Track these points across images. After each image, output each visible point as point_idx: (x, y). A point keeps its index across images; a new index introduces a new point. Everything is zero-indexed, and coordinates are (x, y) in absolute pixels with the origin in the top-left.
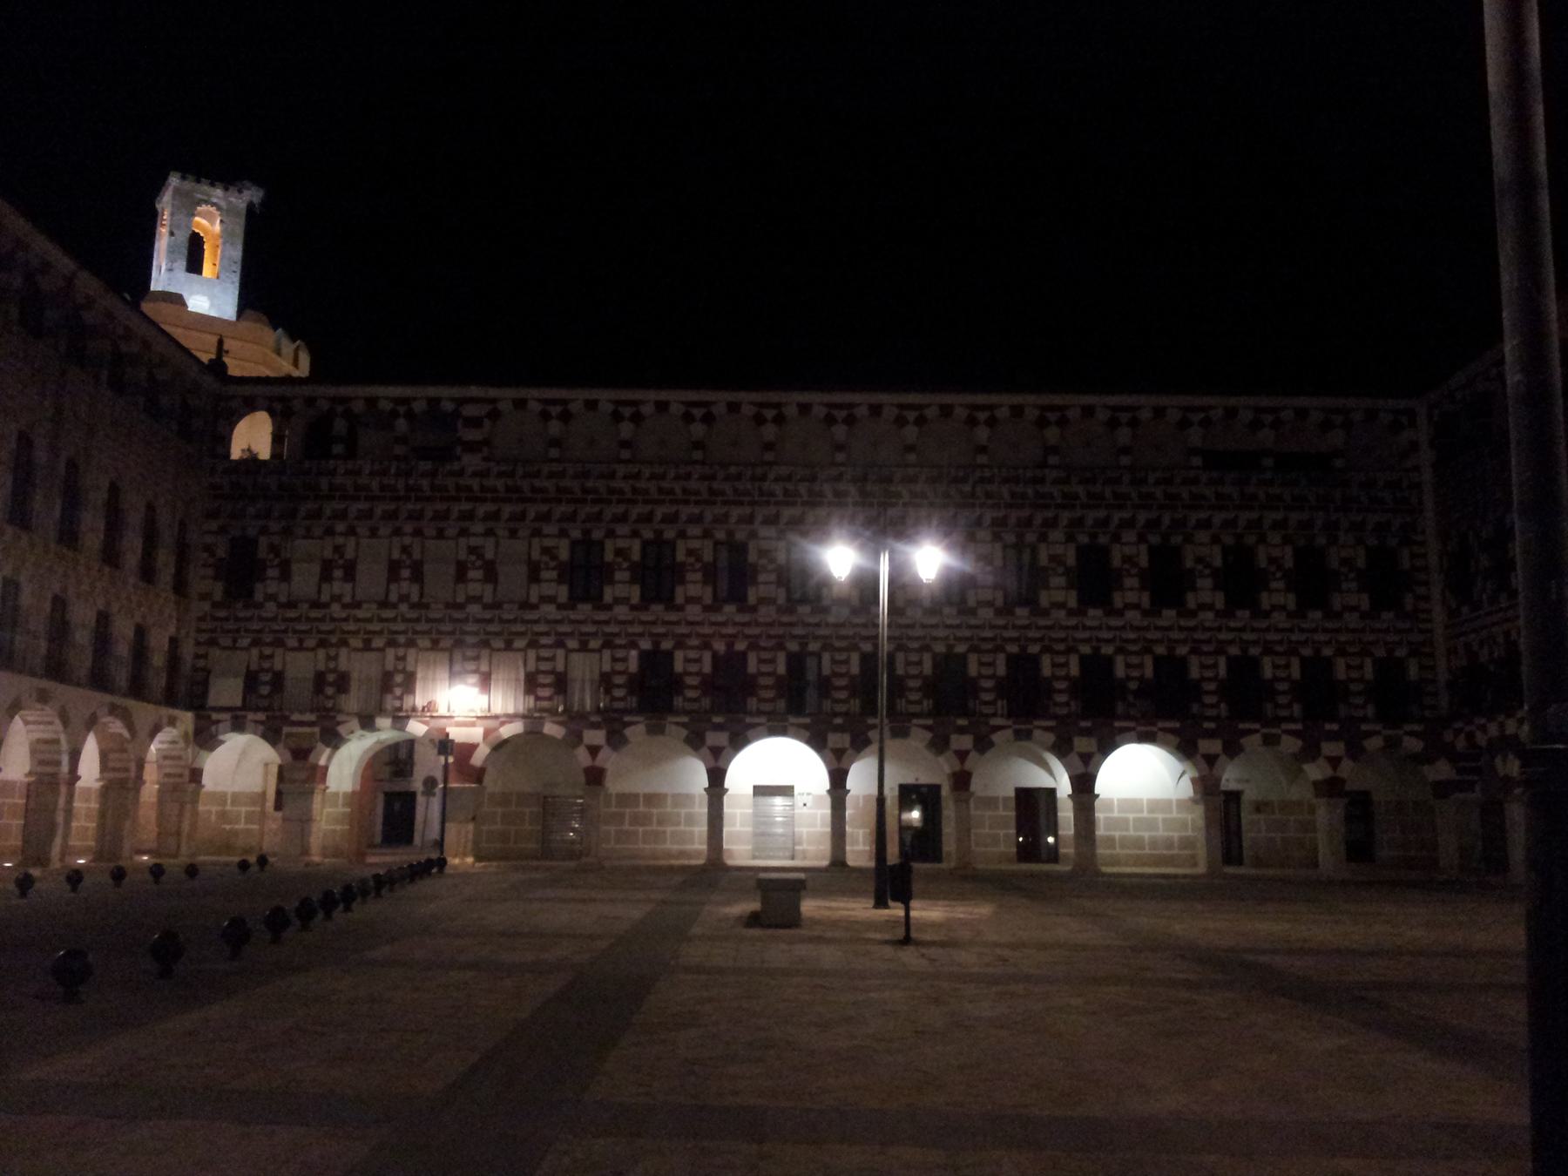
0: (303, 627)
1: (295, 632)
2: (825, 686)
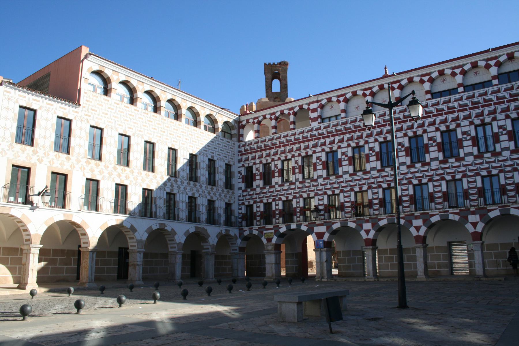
0: (268, 195)
1: (266, 197)
2: (466, 194)
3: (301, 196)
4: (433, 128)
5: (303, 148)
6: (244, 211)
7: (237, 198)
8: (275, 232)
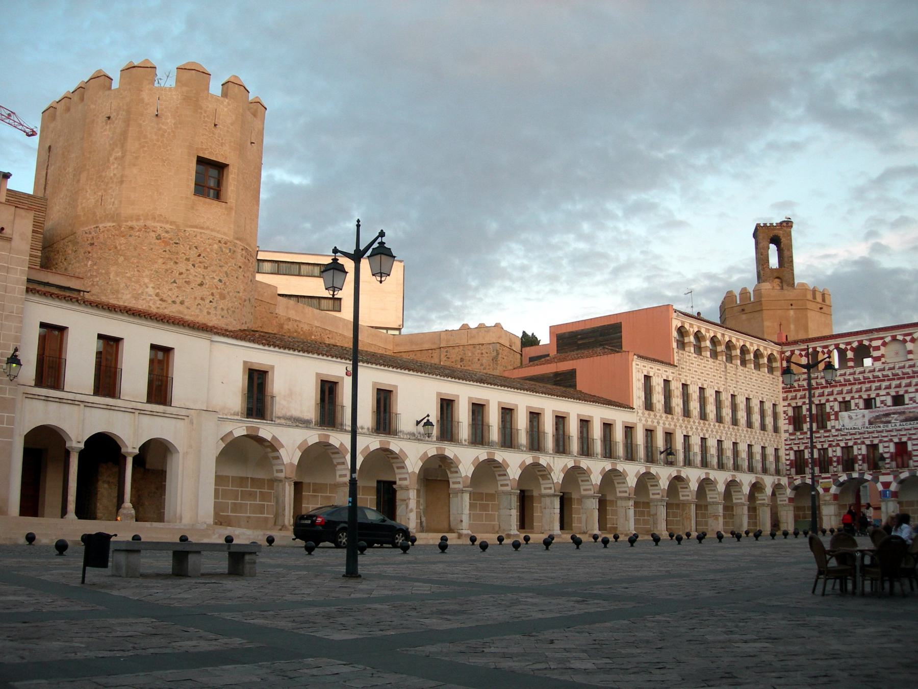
5: (864, 389)
6: (792, 457)
7: (784, 442)
8: (834, 480)
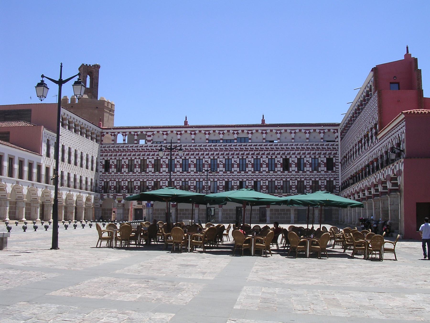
3: (139, 180)
4: (207, 157)
6: (103, 185)
